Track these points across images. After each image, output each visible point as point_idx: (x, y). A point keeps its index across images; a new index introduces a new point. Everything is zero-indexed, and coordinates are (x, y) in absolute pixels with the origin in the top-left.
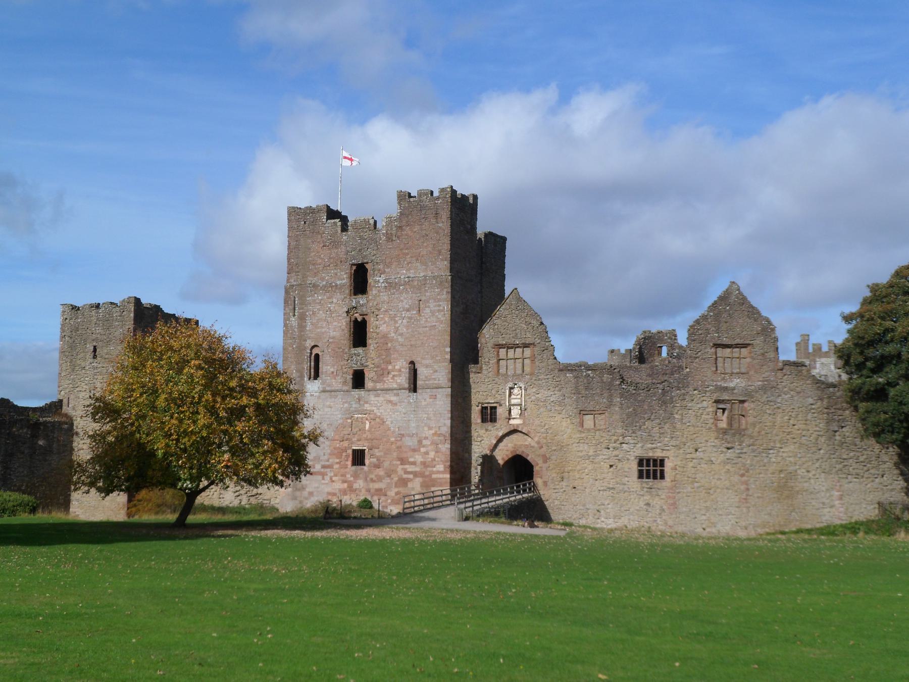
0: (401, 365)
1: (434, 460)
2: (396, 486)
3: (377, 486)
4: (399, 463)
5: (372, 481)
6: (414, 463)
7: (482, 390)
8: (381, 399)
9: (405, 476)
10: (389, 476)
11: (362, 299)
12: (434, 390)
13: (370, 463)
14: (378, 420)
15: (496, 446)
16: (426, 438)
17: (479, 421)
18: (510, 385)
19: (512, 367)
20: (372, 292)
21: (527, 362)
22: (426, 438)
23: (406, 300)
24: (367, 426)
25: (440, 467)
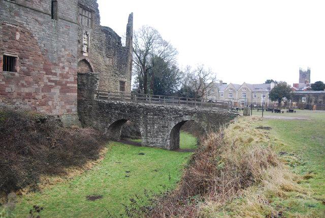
1: (68, 73)
2: (42, 91)
3: (27, 90)
4: (44, 72)
5: (23, 85)
6: (55, 74)
8: (30, 17)
9: (49, 84)
10: (37, 83)
12: (69, 23)
13: (21, 70)
14: (26, 34)
16: (63, 56)
22: (63, 56)
24: (18, 37)
25: (72, 79)
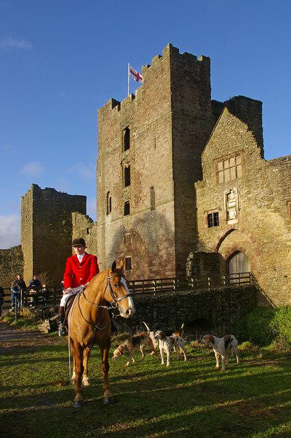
0: (146, 191)
7: (205, 202)
11: (127, 152)
15: (219, 245)
17: (206, 226)
18: (226, 192)
19: (228, 175)
20: (132, 144)
21: (239, 168)
23: (148, 142)
